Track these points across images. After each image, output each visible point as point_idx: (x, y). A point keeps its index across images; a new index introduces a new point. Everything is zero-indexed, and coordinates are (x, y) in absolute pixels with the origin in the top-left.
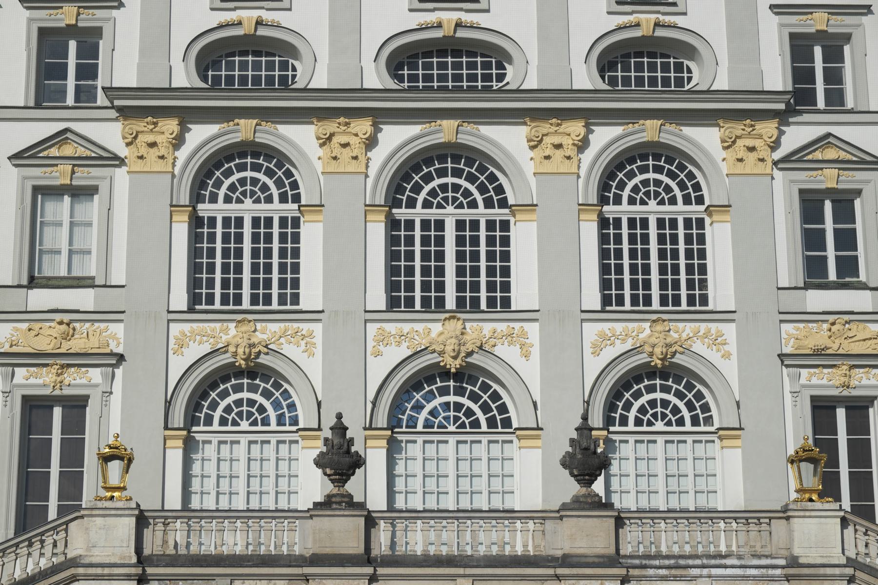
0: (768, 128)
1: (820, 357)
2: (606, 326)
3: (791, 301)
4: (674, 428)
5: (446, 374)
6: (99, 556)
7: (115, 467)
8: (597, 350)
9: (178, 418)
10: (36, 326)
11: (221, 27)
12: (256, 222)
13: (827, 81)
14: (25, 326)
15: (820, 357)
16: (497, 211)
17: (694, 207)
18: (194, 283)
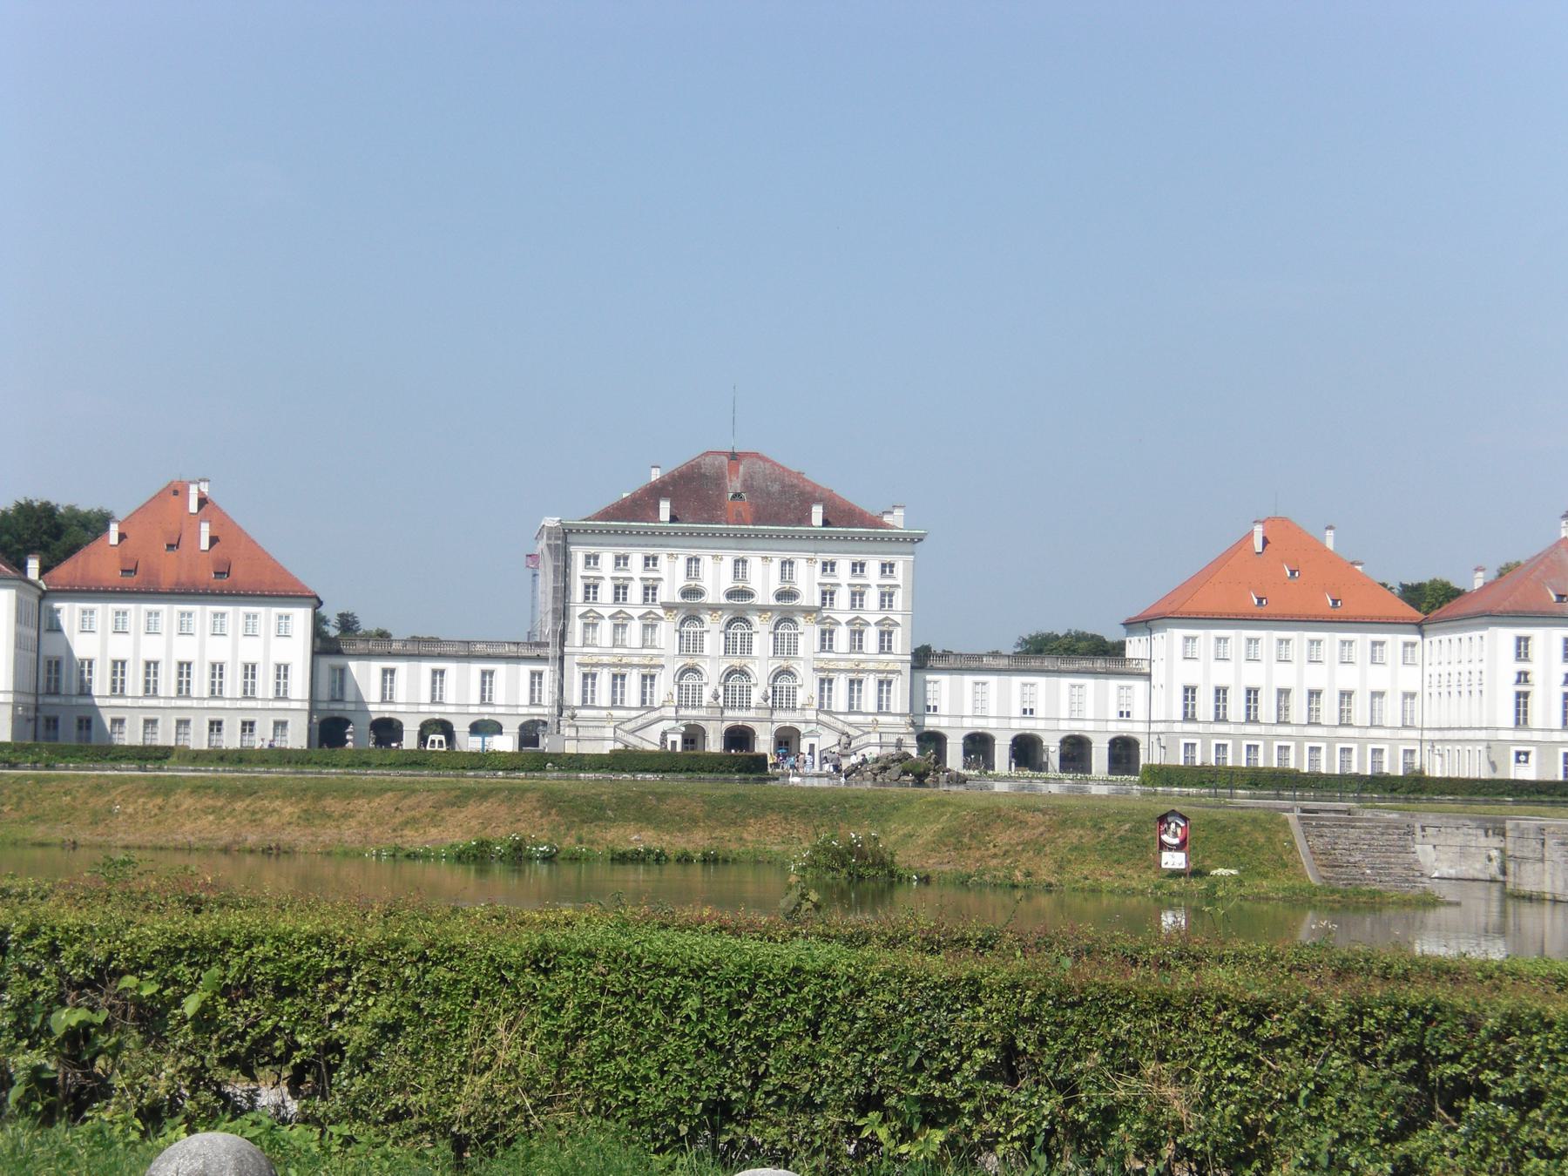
15: (822, 670)
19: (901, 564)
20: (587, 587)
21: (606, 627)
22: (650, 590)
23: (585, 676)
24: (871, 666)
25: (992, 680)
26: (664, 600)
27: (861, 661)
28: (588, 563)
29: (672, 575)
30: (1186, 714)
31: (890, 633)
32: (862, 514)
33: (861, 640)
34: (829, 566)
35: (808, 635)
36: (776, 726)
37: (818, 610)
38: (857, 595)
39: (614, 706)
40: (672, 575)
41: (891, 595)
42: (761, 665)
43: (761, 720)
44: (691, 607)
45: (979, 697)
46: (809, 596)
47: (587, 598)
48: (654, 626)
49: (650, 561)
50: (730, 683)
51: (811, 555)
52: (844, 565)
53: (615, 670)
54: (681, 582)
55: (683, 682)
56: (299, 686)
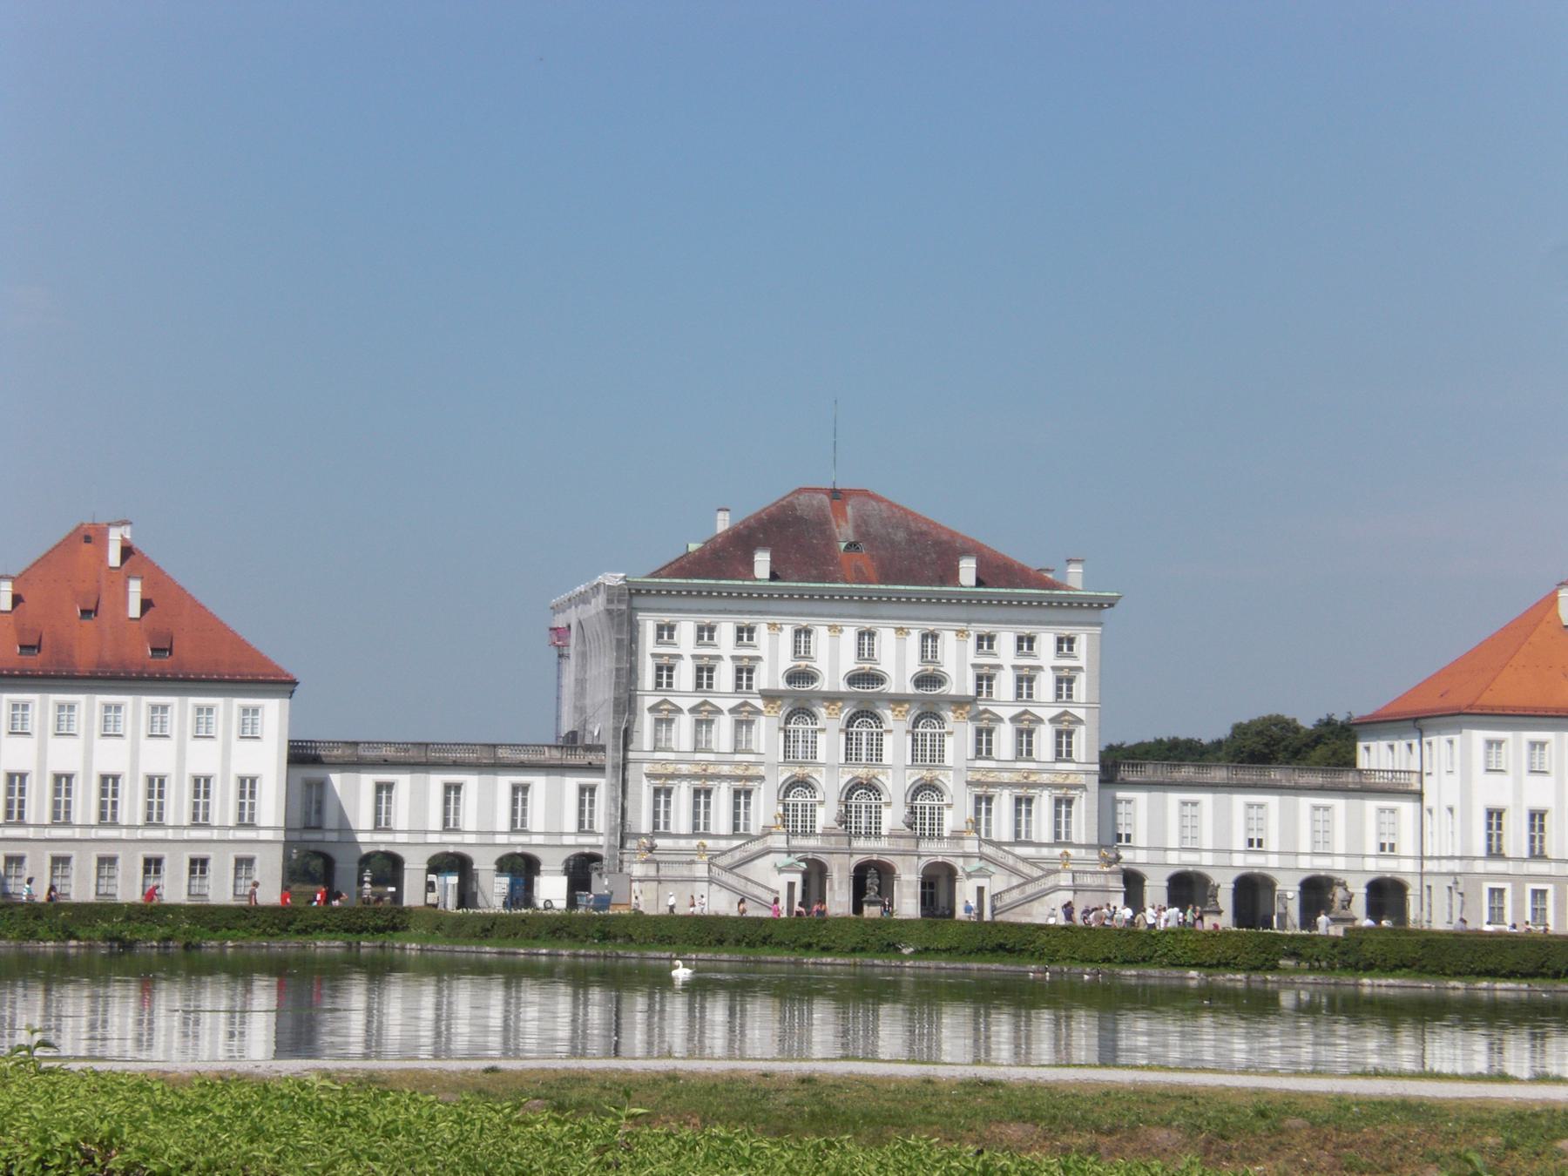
3: (971, 764)
15: (978, 784)
19: (1084, 640)
20: (659, 668)
21: (685, 723)
22: (744, 672)
23: (657, 792)
24: (1045, 778)
25: (1206, 799)
26: (764, 685)
27: (1031, 772)
28: (660, 636)
30: (1489, 847)
31: (1070, 734)
32: (1024, 570)
33: (1030, 743)
34: (985, 642)
35: (958, 738)
36: (924, 862)
37: (972, 701)
38: (1025, 680)
39: (695, 833)
40: (774, 651)
41: (1070, 681)
42: (896, 779)
43: (904, 853)
44: (799, 698)
45: (1188, 822)
46: (960, 682)
47: (659, 684)
48: (749, 723)
49: (744, 633)
51: (962, 626)
52: (1006, 640)
53: (698, 784)
54: (786, 662)
55: (790, 799)
56: (271, 808)
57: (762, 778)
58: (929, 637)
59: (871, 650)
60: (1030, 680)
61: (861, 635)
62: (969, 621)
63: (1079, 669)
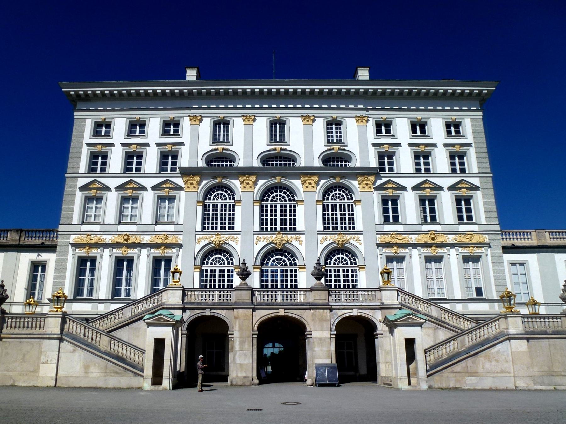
0: (372, 178)
1: (388, 245)
2: (324, 236)
3: (379, 228)
4: (345, 265)
5: (277, 250)
6: (171, 302)
7: (177, 275)
8: (322, 242)
9: (198, 263)
10: (157, 236)
11: (212, 150)
12: (222, 206)
13: (388, 165)
14: (154, 236)
15: (388, 245)
16: (292, 202)
17: (350, 201)
18: (204, 223)
27: (436, 233)
29: (196, 140)
33: (432, 210)
34: (384, 127)
38: (422, 157)
40: (196, 140)
42: (309, 244)
49: (170, 127)
50: (269, 267)
54: (205, 145)
55: (207, 267)
57: (180, 246)
58: (334, 124)
59: (283, 135)
60: (426, 156)
61: (273, 123)
62: (367, 110)
63: (469, 145)
